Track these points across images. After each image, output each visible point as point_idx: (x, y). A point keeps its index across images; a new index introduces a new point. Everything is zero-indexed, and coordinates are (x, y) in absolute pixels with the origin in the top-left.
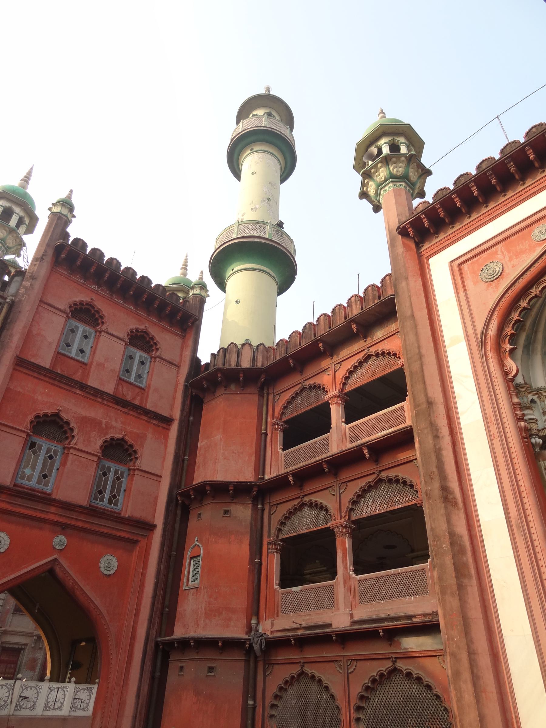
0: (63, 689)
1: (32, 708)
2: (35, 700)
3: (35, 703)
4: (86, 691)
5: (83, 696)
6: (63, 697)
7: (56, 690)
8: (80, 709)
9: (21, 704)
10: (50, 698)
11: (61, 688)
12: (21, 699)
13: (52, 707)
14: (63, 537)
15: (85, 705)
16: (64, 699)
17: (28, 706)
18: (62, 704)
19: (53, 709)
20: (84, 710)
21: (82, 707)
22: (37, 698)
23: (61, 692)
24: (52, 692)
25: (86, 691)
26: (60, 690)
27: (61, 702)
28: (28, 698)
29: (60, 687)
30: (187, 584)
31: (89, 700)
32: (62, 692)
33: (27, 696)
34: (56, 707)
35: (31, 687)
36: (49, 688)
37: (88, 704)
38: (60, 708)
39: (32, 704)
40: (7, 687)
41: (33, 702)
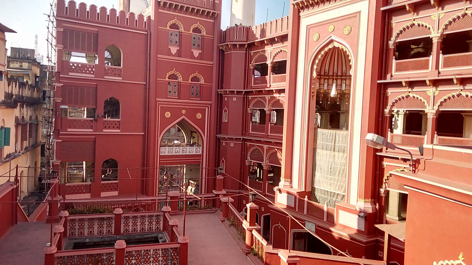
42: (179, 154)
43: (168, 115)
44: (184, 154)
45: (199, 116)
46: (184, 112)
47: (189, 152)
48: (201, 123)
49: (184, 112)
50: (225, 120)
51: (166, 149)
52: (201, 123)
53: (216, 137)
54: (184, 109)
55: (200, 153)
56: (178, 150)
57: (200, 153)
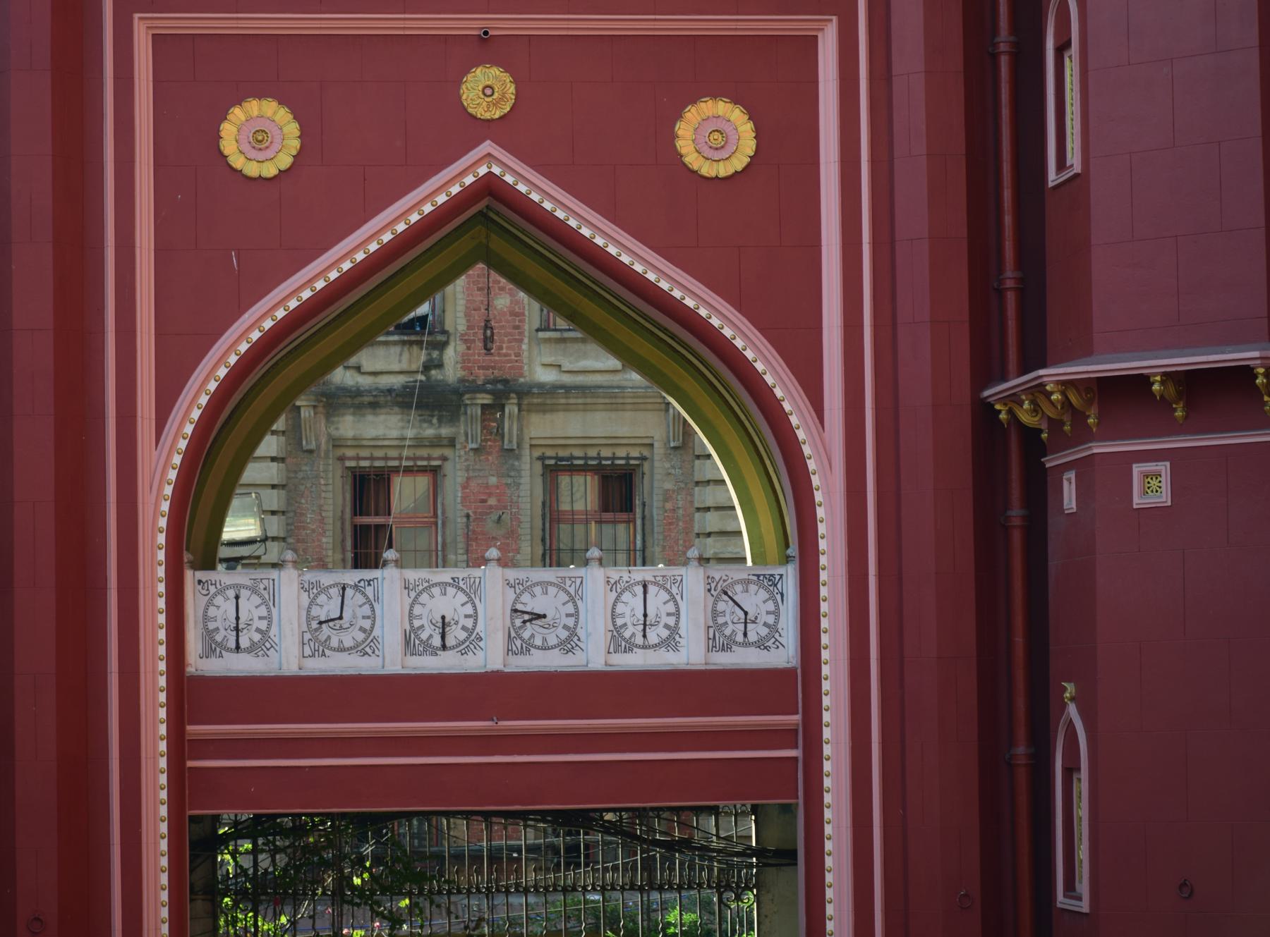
0: (663, 587)
1: (569, 644)
2: (570, 622)
3: (573, 632)
4: (753, 588)
5: (755, 600)
6: (671, 608)
7: (639, 590)
8: (746, 644)
9: (526, 635)
10: (622, 615)
11: (655, 583)
12: (518, 622)
13: (639, 640)
14: (495, 71)
15: (764, 631)
16: (677, 614)
17: (552, 641)
18: (674, 630)
19: (644, 647)
20: (761, 644)
21: (752, 637)
22: (576, 615)
23: (657, 599)
24: (626, 596)
25: (753, 588)
26: (652, 589)
27: (667, 626)
28: (544, 616)
29: (649, 578)
30: (1061, 164)
31: (776, 613)
32: (664, 596)
33: (537, 611)
34: (653, 638)
35: (545, 585)
36: (611, 585)
37: (773, 628)
38: (670, 642)
39: (564, 634)
40: (459, 588)
41: (566, 627)
42: (473, 663)
43: (260, 140)
44: (538, 661)
45: (716, 137)
46: (486, 90)
47: (619, 642)
48: (755, 232)
49: (486, 90)
50: (1067, 150)
51: (270, 600)
52: (755, 232)
53: (984, 412)
54: (486, 48)
55: (785, 655)
56: (449, 604)
57: (785, 655)
